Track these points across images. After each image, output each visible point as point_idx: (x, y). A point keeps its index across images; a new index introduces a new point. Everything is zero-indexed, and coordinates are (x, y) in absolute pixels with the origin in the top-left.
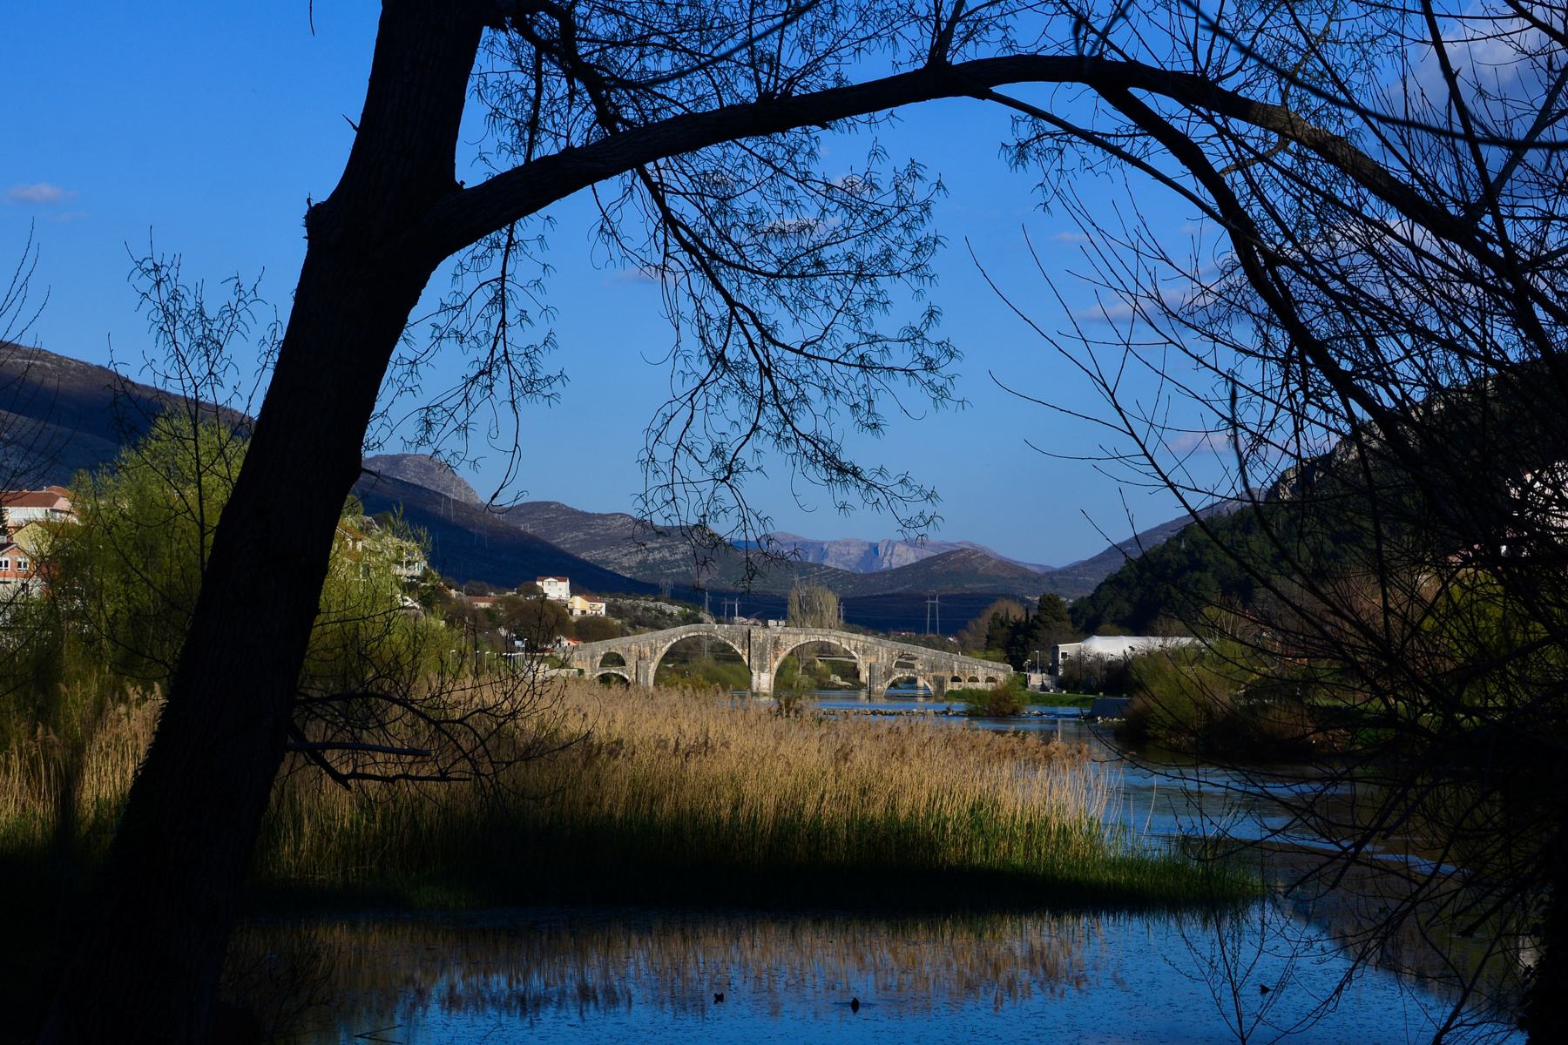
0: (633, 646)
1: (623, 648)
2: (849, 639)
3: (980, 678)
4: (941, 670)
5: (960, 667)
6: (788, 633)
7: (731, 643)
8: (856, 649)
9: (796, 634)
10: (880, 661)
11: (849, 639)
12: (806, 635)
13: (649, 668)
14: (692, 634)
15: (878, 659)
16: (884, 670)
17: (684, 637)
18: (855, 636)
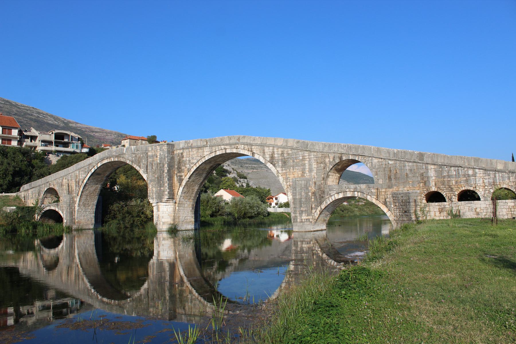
0: (64, 180)
1: (58, 183)
2: (262, 146)
3: (480, 192)
4: (405, 183)
5: (439, 174)
6: (192, 147)
7: (137, 168)
8: (272, 157)
9: (199, 148)
10: (307, 174)
11: (262, 146)
12: (211, 146)
13: (74, 202)
14: (105, 161)
15: (303, 173)
16: (312, 189)
17: (99, 165)
18: (270, 141)
